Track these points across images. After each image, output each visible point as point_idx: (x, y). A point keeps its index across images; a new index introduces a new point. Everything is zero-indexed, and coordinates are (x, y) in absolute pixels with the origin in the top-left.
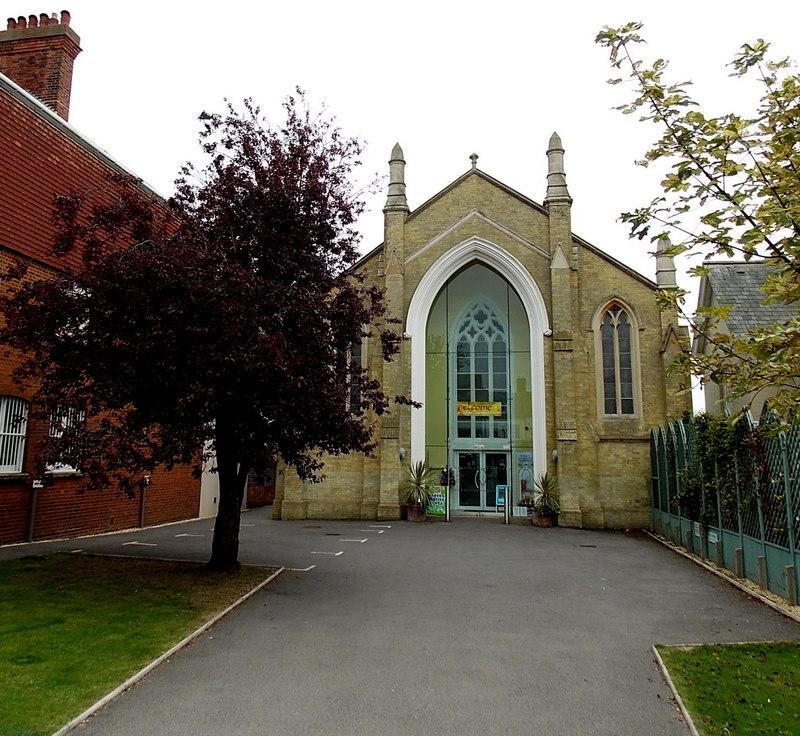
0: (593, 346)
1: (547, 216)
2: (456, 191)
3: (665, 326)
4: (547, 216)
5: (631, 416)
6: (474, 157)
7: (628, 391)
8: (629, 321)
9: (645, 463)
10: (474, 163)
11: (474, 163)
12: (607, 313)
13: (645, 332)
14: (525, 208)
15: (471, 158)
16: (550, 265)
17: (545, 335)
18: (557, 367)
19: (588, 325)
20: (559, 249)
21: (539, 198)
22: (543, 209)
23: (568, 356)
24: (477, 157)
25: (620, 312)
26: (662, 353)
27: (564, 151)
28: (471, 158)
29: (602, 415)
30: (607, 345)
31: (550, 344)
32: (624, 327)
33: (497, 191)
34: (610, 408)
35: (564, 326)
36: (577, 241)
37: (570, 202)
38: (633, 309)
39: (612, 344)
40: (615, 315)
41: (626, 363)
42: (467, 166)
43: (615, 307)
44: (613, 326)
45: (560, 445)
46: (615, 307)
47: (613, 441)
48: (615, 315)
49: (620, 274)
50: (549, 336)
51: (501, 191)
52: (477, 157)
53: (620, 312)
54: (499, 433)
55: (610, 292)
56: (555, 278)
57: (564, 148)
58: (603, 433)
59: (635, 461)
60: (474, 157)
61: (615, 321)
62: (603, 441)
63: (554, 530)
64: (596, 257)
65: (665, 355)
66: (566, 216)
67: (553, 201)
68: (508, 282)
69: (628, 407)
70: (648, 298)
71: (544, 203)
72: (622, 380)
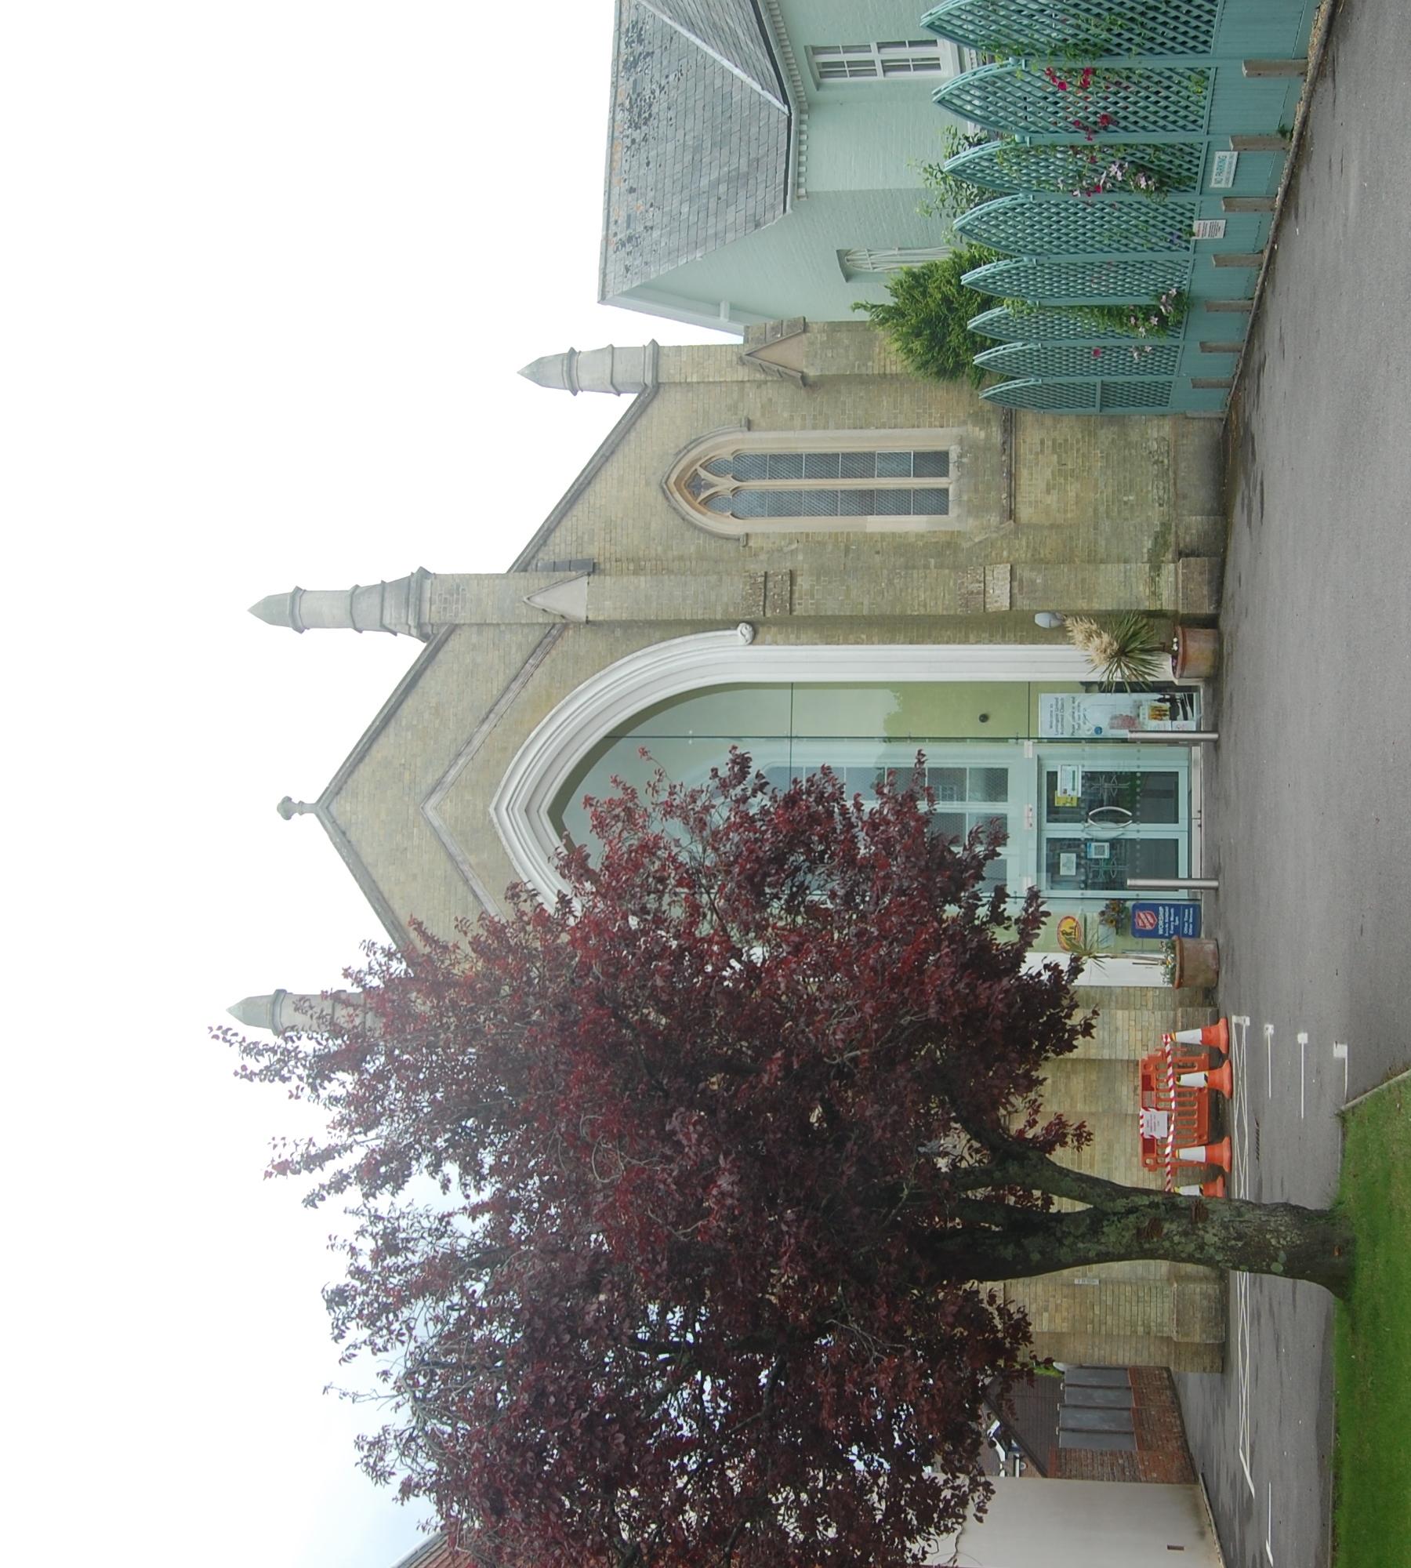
0: (784, 536)
1: (454, 628)
2: (368, 854)
3: (742, 374)
4: (454, 628)
5: (953, 457)
6: (287, 808)
7: (895, 463)
8: (726, 453)
9: (1067, 428)
10: (302, 808)
11: (302, 808)
12: (706, 502)
13: (756, 416)
14: (427, 682)
15: (288, 817)
16: (577, 624)
17: (751, 643)
18: (831, 608)
19: (730, 546)
20: (539, 601)
21: (409, 649)
22: (436, 640)
23: (803, 583)
24: (287, 800)
25: (703, 473)
26: (804, 378)
27: (298, 589)
28: (288, 817)
29: (952, 521)
30: (782, 506)
31: (774, 629)
32: (744, 466)
33: (378, 752)
34: (937, 502)
35: (732, 591)
36: (524, 564)
37: (423, 573)
38: (697, 442)
39: (778, 495)
40: (712, 486)
41: (825, 464)
42: (310, 828)
43: (692, 485)
44: (736, 491)
45: (1023, 603)
46: (692, 485)
47: (1012, 496)
48: (712, 486)
49: (612, 470)
50: (755, 633)
51: (382, 740)
52: (288, 800)
53: (703, 473)
54: (996, 783)
55: (654, 496)
56: (608, 611)
57: (290, 590)
58: (994, 519)
59: (1058, 447)
60: (287, 808)
61: (725, 484)
62: (1011, 514)
63: (1222, 623)
64: (567, 523)
65: (812, 372)
66: (458, 586)
67: (419, 614)
68: (612, 738)
69: (935, 462)
70: (669, 411)
71: (423, 637)
72: (868, 473)
